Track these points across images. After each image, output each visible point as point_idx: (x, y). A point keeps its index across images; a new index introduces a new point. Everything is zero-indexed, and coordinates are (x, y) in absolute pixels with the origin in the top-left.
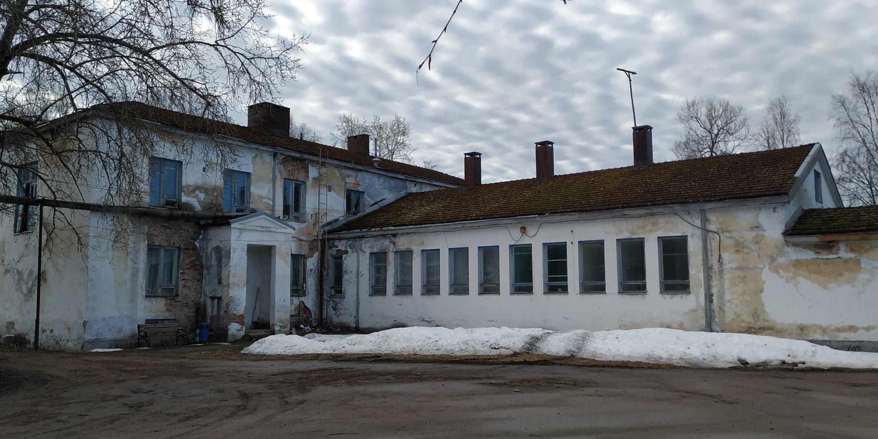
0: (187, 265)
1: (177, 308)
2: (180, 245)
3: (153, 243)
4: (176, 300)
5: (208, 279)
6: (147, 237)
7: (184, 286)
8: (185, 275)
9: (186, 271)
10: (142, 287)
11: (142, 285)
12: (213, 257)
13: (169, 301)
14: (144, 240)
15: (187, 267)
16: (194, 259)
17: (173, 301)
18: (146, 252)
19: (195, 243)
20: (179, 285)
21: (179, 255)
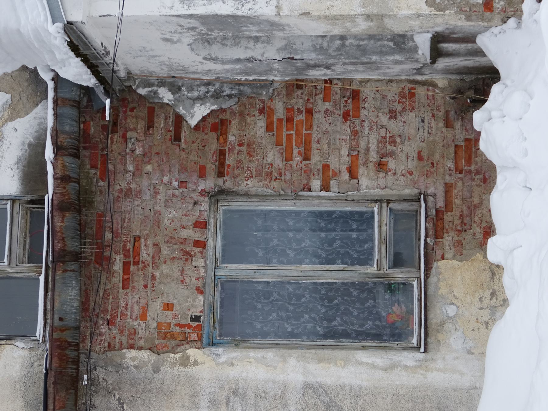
0: (289, 158)
1: (476, 200)
2: (204, 193)
3: (196, 319)
4: (441, 204)
5: (350, 67)
6: (173, 351)
7: (381, 166)
8: (334, 164)
9: (316, 159)
10: (385, 369)
11: (373, 366)
12: (249, 54)
13: (448, 239)
14: (185, 362)
15: (297, 158)
16: (261, 123)
17: (448, 217)
18: (235, 354)
19: (193, 122)
20: (377, 192)
21: (247, 195)
